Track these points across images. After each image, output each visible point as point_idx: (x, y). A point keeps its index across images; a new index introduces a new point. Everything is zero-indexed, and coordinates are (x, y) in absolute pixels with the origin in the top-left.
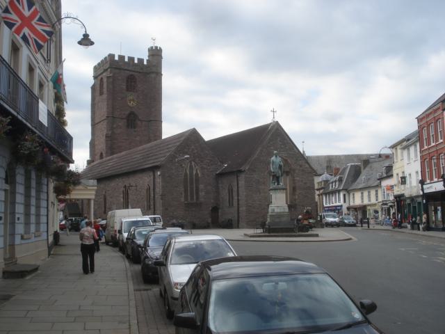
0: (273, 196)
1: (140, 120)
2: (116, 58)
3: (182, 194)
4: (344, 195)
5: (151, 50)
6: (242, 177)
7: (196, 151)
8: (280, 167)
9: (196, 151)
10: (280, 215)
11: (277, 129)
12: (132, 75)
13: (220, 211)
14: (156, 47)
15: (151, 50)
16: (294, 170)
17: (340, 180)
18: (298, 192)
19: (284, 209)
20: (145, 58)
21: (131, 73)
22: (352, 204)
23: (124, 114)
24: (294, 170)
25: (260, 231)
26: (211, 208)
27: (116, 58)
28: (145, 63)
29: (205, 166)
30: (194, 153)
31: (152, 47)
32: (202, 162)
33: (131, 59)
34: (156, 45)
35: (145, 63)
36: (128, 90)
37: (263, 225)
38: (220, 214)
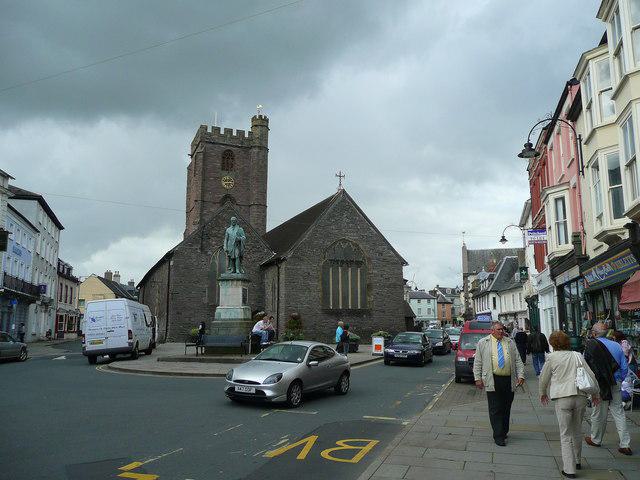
0: (222, 291)
4: (494, 298)
5: (254, 119)
6: (283, 266)
8: (238, 243)
10: (228, 325)
11: (344, 201)
14: (261, 116)
16: (369, 259)
17: (491, 278)
18: (375, 290)
20: (246, 127)
21: (229, 148)
22: (504, 311)
24: (369, 259)
25: (192, 350)
28: (247, 136)
33: (229, 131)
35: (247, 136)
37: (197, 340)
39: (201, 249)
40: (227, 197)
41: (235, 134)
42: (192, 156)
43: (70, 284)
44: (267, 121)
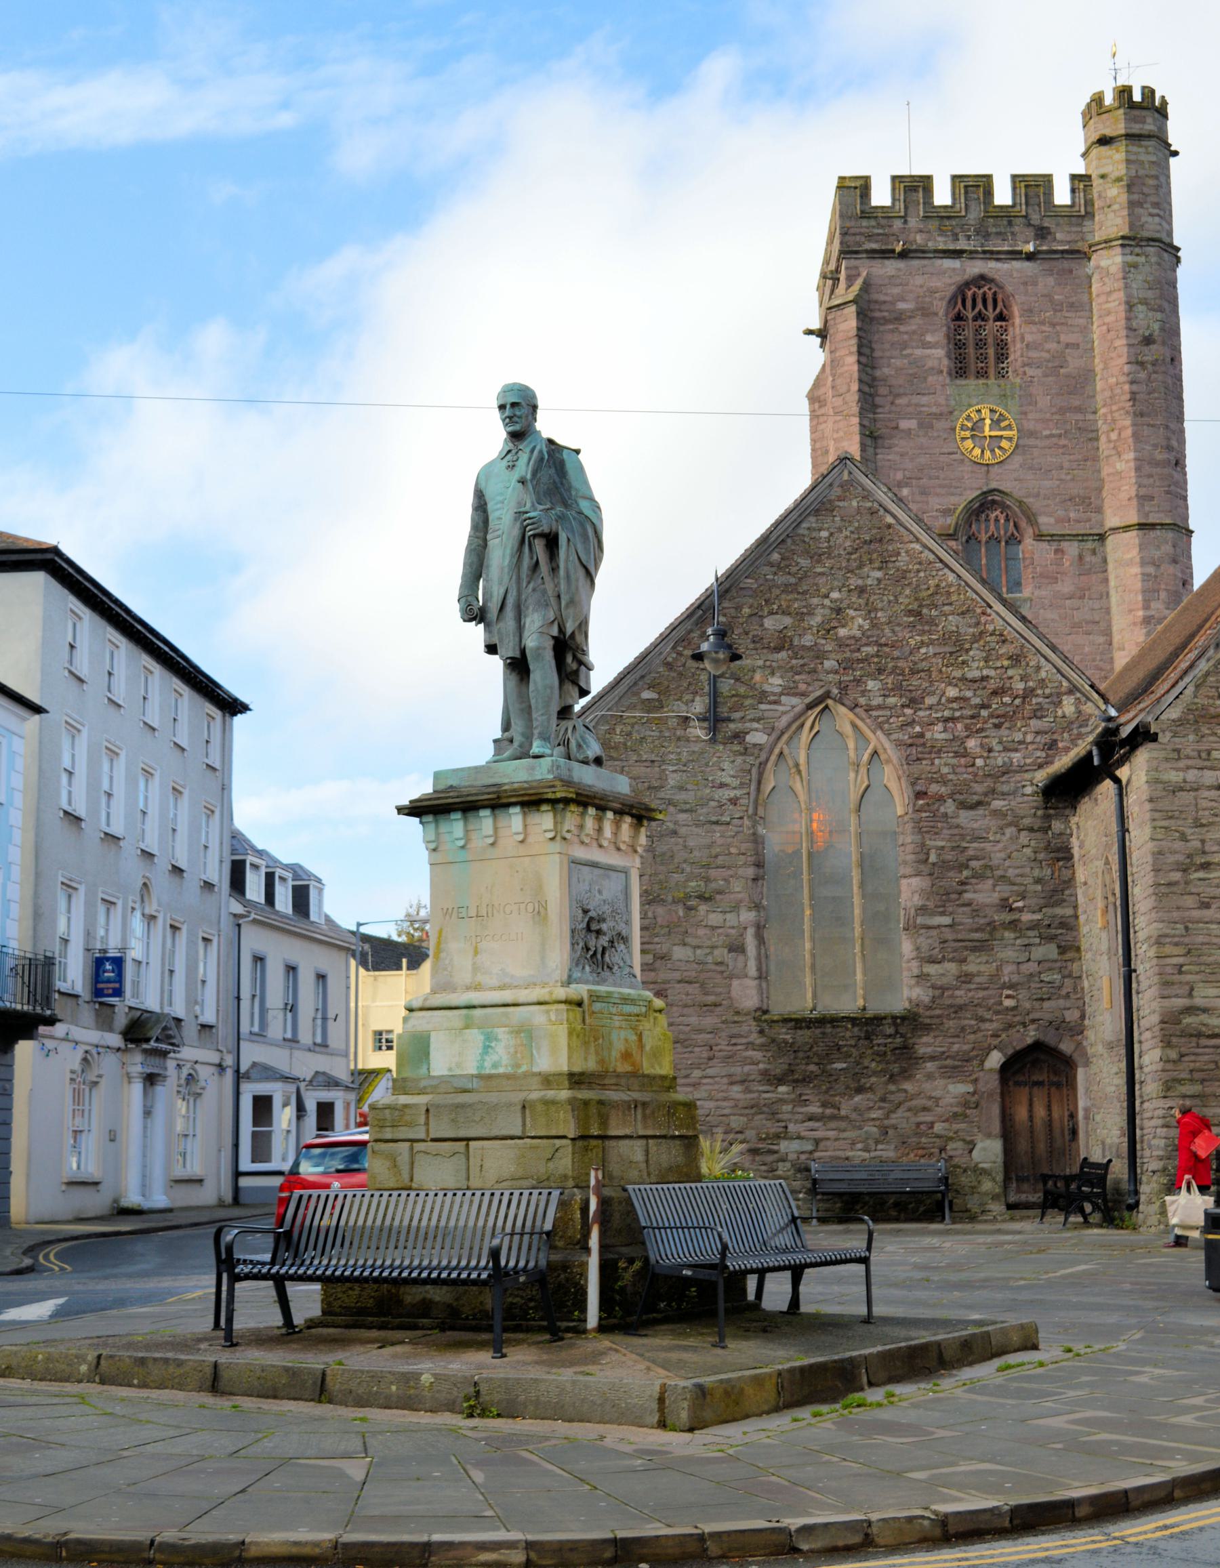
1: (1039, 537)
2: (881, 196)
3: (737, 948)
7: (856, 624)
9: (856, 624)
12: (982, 279)
13: (1081, 1073)
14: (1124, 92)
15: (1096, 106)
19: (525, 1033)
21: (976, 267)
23: (947, 512)
26: (995, 1059)
27: (881, 196)
29: (937, 733)
30: (841, 644)
31: (1098, 99)
32: (914, 702)
34: (1122, 81)
35: (1062, 195)
36: (960, 370)
38: (1081, 1104)
39: (714, 720)
40: (985, 504)
41: (1003, 196)
42: (822, 334)
43: (310, 960)
44: (1162, 112)
